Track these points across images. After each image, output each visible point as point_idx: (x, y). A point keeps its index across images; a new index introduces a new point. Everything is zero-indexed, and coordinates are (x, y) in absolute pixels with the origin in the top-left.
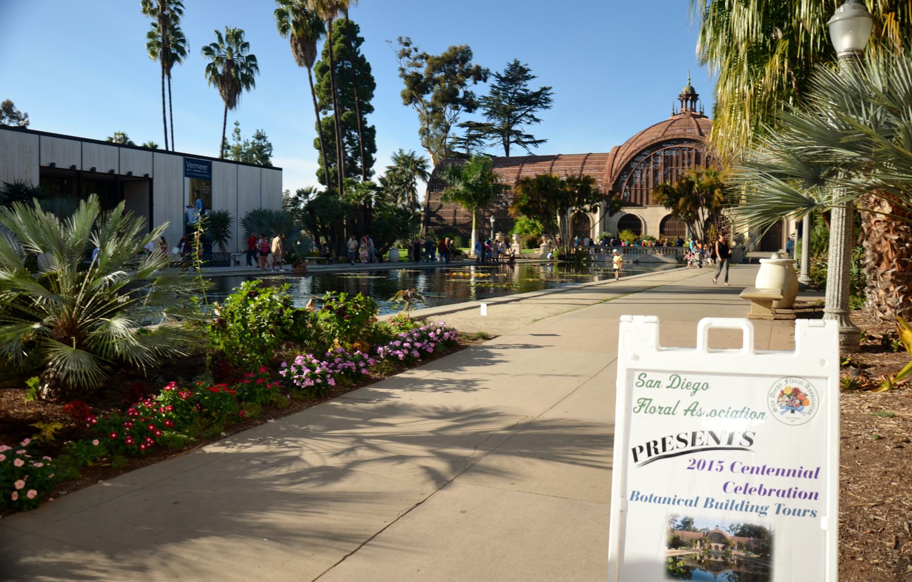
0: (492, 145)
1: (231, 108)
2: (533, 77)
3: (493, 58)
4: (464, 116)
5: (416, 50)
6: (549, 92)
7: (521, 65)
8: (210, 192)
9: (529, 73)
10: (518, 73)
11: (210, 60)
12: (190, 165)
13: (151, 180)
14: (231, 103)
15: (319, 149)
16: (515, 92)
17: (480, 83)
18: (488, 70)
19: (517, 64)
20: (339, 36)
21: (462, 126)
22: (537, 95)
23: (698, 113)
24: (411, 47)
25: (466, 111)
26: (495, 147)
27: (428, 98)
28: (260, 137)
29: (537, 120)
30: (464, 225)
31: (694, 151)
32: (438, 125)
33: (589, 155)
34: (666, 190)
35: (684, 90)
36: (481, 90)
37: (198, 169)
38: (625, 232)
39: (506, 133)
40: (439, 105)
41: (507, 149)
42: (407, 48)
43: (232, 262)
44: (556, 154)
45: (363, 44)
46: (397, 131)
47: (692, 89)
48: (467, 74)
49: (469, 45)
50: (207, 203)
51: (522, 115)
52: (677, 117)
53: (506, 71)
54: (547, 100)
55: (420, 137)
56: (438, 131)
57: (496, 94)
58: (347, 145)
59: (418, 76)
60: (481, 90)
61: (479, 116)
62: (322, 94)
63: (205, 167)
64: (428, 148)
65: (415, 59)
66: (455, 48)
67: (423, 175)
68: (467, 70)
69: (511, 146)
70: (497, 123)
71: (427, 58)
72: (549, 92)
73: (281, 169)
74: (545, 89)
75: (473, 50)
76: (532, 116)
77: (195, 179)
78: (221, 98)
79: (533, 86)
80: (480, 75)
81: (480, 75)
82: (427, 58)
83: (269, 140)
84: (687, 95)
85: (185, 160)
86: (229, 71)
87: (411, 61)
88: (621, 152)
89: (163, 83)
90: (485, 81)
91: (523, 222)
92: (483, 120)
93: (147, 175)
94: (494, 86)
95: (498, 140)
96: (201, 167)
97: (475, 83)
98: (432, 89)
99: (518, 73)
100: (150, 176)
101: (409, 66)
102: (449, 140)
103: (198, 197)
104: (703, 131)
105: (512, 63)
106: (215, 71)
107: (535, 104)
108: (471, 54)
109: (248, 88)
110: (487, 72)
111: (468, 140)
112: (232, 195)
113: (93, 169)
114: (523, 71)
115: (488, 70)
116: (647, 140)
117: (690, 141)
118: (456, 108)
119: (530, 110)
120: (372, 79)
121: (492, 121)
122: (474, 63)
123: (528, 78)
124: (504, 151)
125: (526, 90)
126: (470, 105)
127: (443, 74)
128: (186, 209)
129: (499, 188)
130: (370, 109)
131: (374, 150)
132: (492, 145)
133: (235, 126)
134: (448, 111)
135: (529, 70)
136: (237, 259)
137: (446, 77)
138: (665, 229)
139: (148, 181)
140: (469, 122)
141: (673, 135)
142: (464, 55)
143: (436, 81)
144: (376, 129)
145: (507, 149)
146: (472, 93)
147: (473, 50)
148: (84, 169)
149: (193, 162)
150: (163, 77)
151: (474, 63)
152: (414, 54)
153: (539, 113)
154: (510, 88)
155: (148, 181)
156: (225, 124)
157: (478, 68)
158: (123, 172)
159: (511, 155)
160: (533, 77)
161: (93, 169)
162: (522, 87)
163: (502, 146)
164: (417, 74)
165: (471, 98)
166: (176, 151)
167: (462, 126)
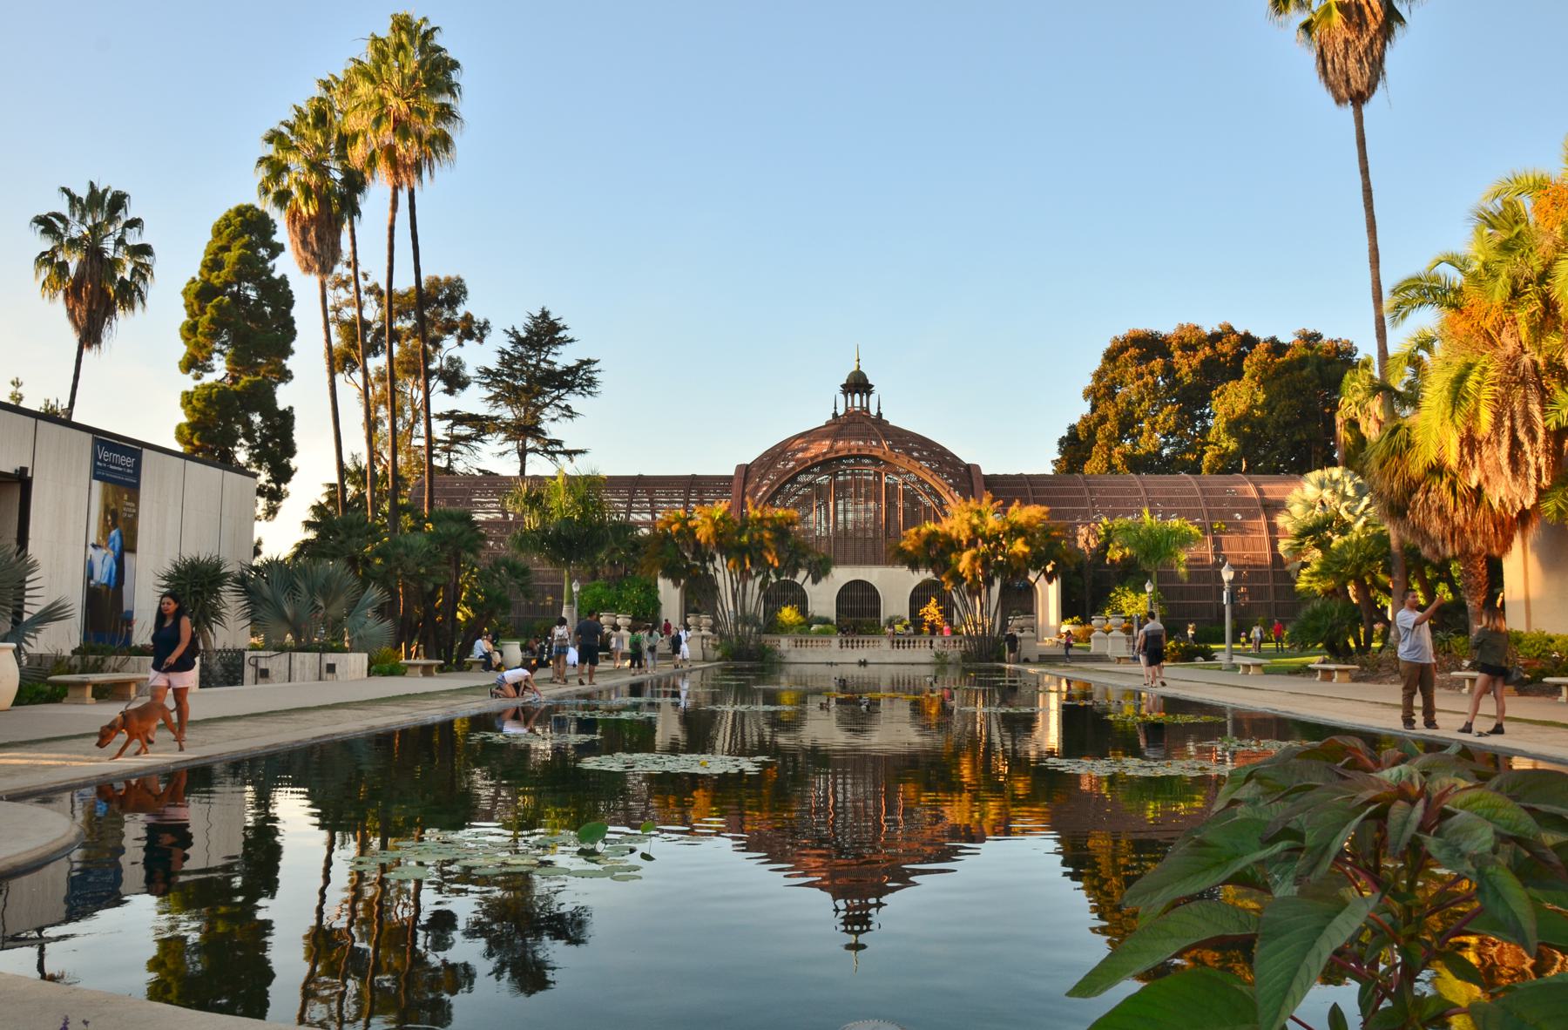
0: (502, 454)
1: (89, 346)
3: (500, 307)
4: (441, 402)
7: (552, 317)
8: (136, 515)
9: (561, 334)
10: (544, 332)
11: (47, 244)
12: (105, 455)
14: (90, 335)
16: (537, 366)
19: (545, 315)
20: (241, 235)
22: (569, 371)
27: (377, 363)
39: (525, 431)
43: (249, 672)
45: (282, 255)
48: (450, 327)
54: (591, 382)
58: (242, 440)
60: (477, 357)
61: (473, 400)
66: (437, 279)
69: (529, 456)
70: (507, 413)
72: (593, 368)
74: (589, 362)
76: (567, 408)
79: (563, 358)
80: (471, 330)
81: (471, 330)
85: (96, 442)
90: (480, 341)
92: (483, 410)
93: (24, 470)
94: (503, 352)
97: (461, 344)
103: (115, 525)
105: (537, 314)
107: (570, 387)
110: (485, 326)
114: (554, 328)
119: (559, 397)
120: (292, 321)
121: (494, 413)
123: (562, 341)
126: (455, 380)
130: (286, 376)
131: (291, 451)
132: (502, 454)
133: (13, 389)
134: (412, 390)
136: (262, 665)
142: (455, 292)
143: (395, 336)
144: (296, 413)
146: (459, 360)
151: (461, 311)
153: (572, 400)
154: (530, 357)
156: (76, 377)
157: (468, 318)
162: (550, 358)
163: (517, 457)
166: (75, 419)
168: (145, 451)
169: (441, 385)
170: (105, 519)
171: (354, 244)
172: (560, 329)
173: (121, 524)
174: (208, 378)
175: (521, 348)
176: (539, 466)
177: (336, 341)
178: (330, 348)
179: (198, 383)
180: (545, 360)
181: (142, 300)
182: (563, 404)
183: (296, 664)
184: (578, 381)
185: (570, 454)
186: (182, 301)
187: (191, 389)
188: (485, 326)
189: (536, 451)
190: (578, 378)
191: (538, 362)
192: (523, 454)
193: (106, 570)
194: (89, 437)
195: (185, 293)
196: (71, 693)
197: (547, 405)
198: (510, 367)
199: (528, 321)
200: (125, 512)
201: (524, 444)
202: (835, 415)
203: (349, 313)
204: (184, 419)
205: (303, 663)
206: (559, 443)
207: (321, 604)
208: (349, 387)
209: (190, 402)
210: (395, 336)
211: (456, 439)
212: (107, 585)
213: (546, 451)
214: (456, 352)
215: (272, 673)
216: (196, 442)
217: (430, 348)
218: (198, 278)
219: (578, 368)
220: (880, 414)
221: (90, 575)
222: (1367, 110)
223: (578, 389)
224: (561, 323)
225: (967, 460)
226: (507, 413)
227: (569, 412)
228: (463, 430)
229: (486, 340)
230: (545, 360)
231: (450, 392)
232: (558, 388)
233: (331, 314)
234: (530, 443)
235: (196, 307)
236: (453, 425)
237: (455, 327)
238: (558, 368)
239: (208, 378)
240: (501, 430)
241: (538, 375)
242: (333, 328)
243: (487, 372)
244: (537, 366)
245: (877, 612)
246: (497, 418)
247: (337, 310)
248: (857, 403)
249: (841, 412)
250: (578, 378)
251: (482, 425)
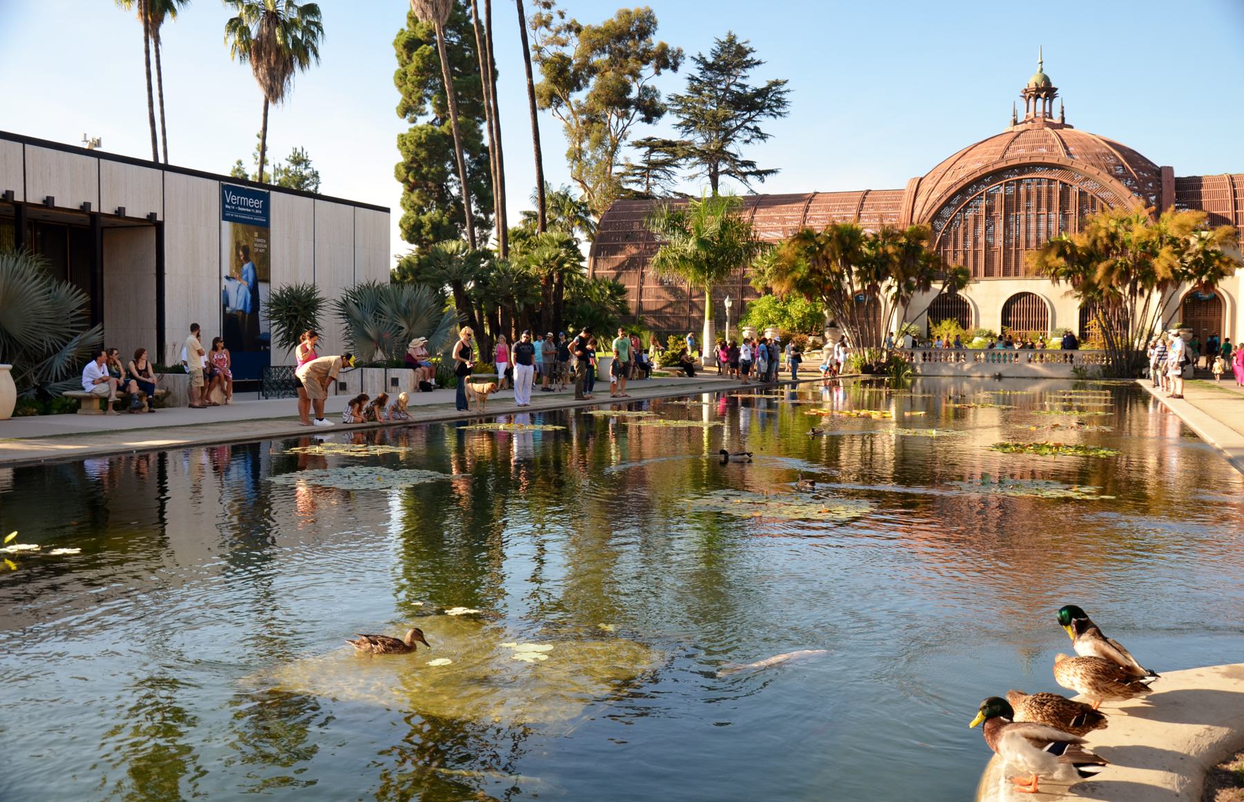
0: (692, 178)
1: (274, 101)
2: (758, 63)
3: (690, 33)
4: (639, 129)
5: (562, 15)
6: (782, 89)
8: (268, 250)
9: (749, 58)
10: (733, 56)
12: (231, 198)
13: (160, 227)
14: (274, 91)
15: (405, 181)
16: (727, 90)
17: (666, 73)
18: (680, 51)
19: (732, 41)
21: (639, 145)
22: (762, 93)
23: (1056, 119)
24: (554, 9)
25: (642, 120)
26: (697, 179)
27: (579, 97)
28: (298, 160)
29: (763, 137)
30: (656, 311)
31: (1057, 187)
32: (600, 142)
33: (868, 192)
34: (1062, 249)
35: (1033, 80)
36: (669, 85)
37: (246, 201)
38: (946, 324)
39: (715, 158)
40: (600, 109)
41: (715, 185)
42: (545, 12)
44: (807, 189)
46: (536, 155)
47: (1046, 79)
48: (644, 58)
49: (651, 7)
50: (262, 274)
51: (738, 128)
52: (1020, 128)
53: (714, 53)
54: (780, 103)
55: (568, 163)
56: (600, 153)
57: (698, 92)
58: (452, 176)
59: (564, 61)
60: (669, 85)
61: (667, 128)
62: (409, 86)
63: (258, 203)
64: (582, 182)
65: (558, 32)
66: (629, 13)
67: (585, 225)
68: (645, 50)
69: (721, 178)
70: (698, 139)
71: (578, 30)
73: (387, 210)
74: (776, 83)
75: (658, 17)
76: (756, 129)
77: (239, 226)
78: (257, 83)
79: (755, 79)
80: (666, 60)
81: (666, 60)
82: (578, 30)
83: (314, 166)
84: (1038, 90)
85: (223, 188)
86: (271, 34)
87: (551, 35)
88: (925, 187)
89: (147, 52)
90: (675, 69)
91: (765, 306)
92: (675, 136)
93: (152, 216)
94: (692, 79)
95: (703, 169)
96: (250, 201)
97: (658, 73)
98: (586, 82)
99: (733, 56)
100: (159, 218)
101: (547, 43)
102: (616, 169)
103: (247, 259)
104: (1071, 149)
105: (724, 38)
106: (245, 31)
108: (655, 24)
109: (302, 65)
110: (679, 55)
111: (648, 170)
112: (299, 255)
113: (49, 201)
114: (741, 52)
115: (680, 51)
116: (973, 166)
117: (1051, 167)
118: (626, 115)
119: (750, 119)
121: (686, 139)
122: (656, 40)
123: (749, 64)
124: (710, 188)
125: (743, 86)
126: (652, 112)
127: (607, 56)
128: (225, 281)
129: (754, 246)
132: (692, 178)
135: (751, 50)
137: (612, 63)
138: (1011, 319)
139: (155, 225)
140: (650, 139)
141: (1021, 157)
142: (644, 25)
143: (593, 70)
145: (715, 185)
147: (658, 17)
148: (30, 200)
149: (237, 192)
150: (147, 41)
151: (656, 40)
152: (557, 22)
153: (765, 122)
154: (719, 82)
155: (155, 225)
157: (664, 49)
158: (108, 209)
159: (722, 192)
160: (758, 63)
161: (49, 201)
162: (739, 81)
163: (708, 179)
164: (562, 57)
165: (652, 99)
167: (639, 145)
168: (273, 193)
169: (639, 115)
170: (237, 254)
172: (747, 52)
173: (252, 257)
174: (422, 121)
175: (709, 74)
176: (731, 187)
177: (539, 78)
178: (531, 86)
179: (413, 126)
181: (317, 56)
183: (367, 379)
185: (759, 173)
186: (393, 52)
187: (405, 131)
188: (679, 55)
192: (714, 178)
193: (241, 298)
194: (215, 184)
195: (395, 44)
196: (83, 405)
197: (738, 128)
198: (699, 92)
199: (716, 47)
200: (256, 245)
201: (716, 168)
203: (550, 51)
204: (401, 159)
205: (372, 377)
206: (751, 164)
207: (403, 324)
208: (554, 123)
209: (405, 144)
210: (593, 70)
211: (655, 165)
212: (243, 311)
215: (349, 386)
216: (411, 179)
217: (630, 78)
218: (406, 29)
219: (768, 89)
221: (226, 304)
223: (767, 111)
224: (747, 47)
225: (1159, 163)
226: (698, 139)
228: (658, 156)
229: (680, 68)
231: (648, 120)
232: (749, 110)
233: (533, 54)
234: (723, 167)
235: (405, 57)
236: (652, 151)
238: (749, 90)
239: (422, 121)
240: (689, 155)
241: (733, 98)
242: (536, 67)
243: (678, 99)
244: (727, 90)
246: (689, 143)
247: (539, 49)
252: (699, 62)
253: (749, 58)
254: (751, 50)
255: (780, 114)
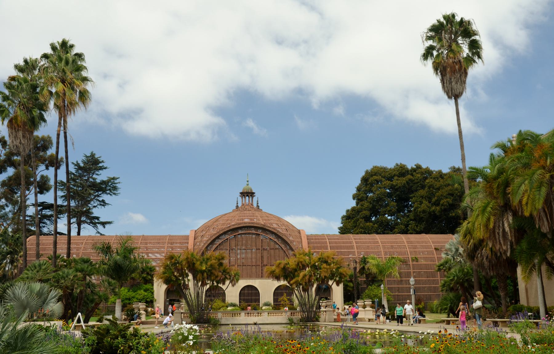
7: (96, 156)
9: (101, 165)
10: (93, 164)
19: (93, 155)
22: (103, 182)
54: (115, 188)
69: (83, 226)
74: (114, 179)
76: (103, 201)
79: (101, 177)
105: (89, 155)
107: (104, 191)
119: (98, 196)
123: (102, 168)
125: (94, 179)
135: (103, 162)
146: (47, 177)
153: (105, 197)
154: (85, 176)
160: (105, 168)
162: (94, 176)
171: (66, 152)
172: (100, 162)
180: (92, 177)
182: (101, 199)
184: (108, 188)
189: (87, 223)
190: (109, 186)
191: (88, 178)
197: (92, 200)
199: (84, 158)
202: (237, 207)
206: (98, 218)
213: (91, 223)
214: (45, 173)
219: (109, 181)
220: (258, 206)
222: (459, 101)
223: (108, 192)
227: (103, 203)
228: (48, 212)
230: (92, 177)
232: (98, 191)
237: (45, 160)
245: (258, 300)
248: (247, 201)
249: (240, 205)
250: (109, 186)
251: (59, 210)
252: (76, 165)
253: (101, 165)
254: (103, 162)
255: (114, 194)
